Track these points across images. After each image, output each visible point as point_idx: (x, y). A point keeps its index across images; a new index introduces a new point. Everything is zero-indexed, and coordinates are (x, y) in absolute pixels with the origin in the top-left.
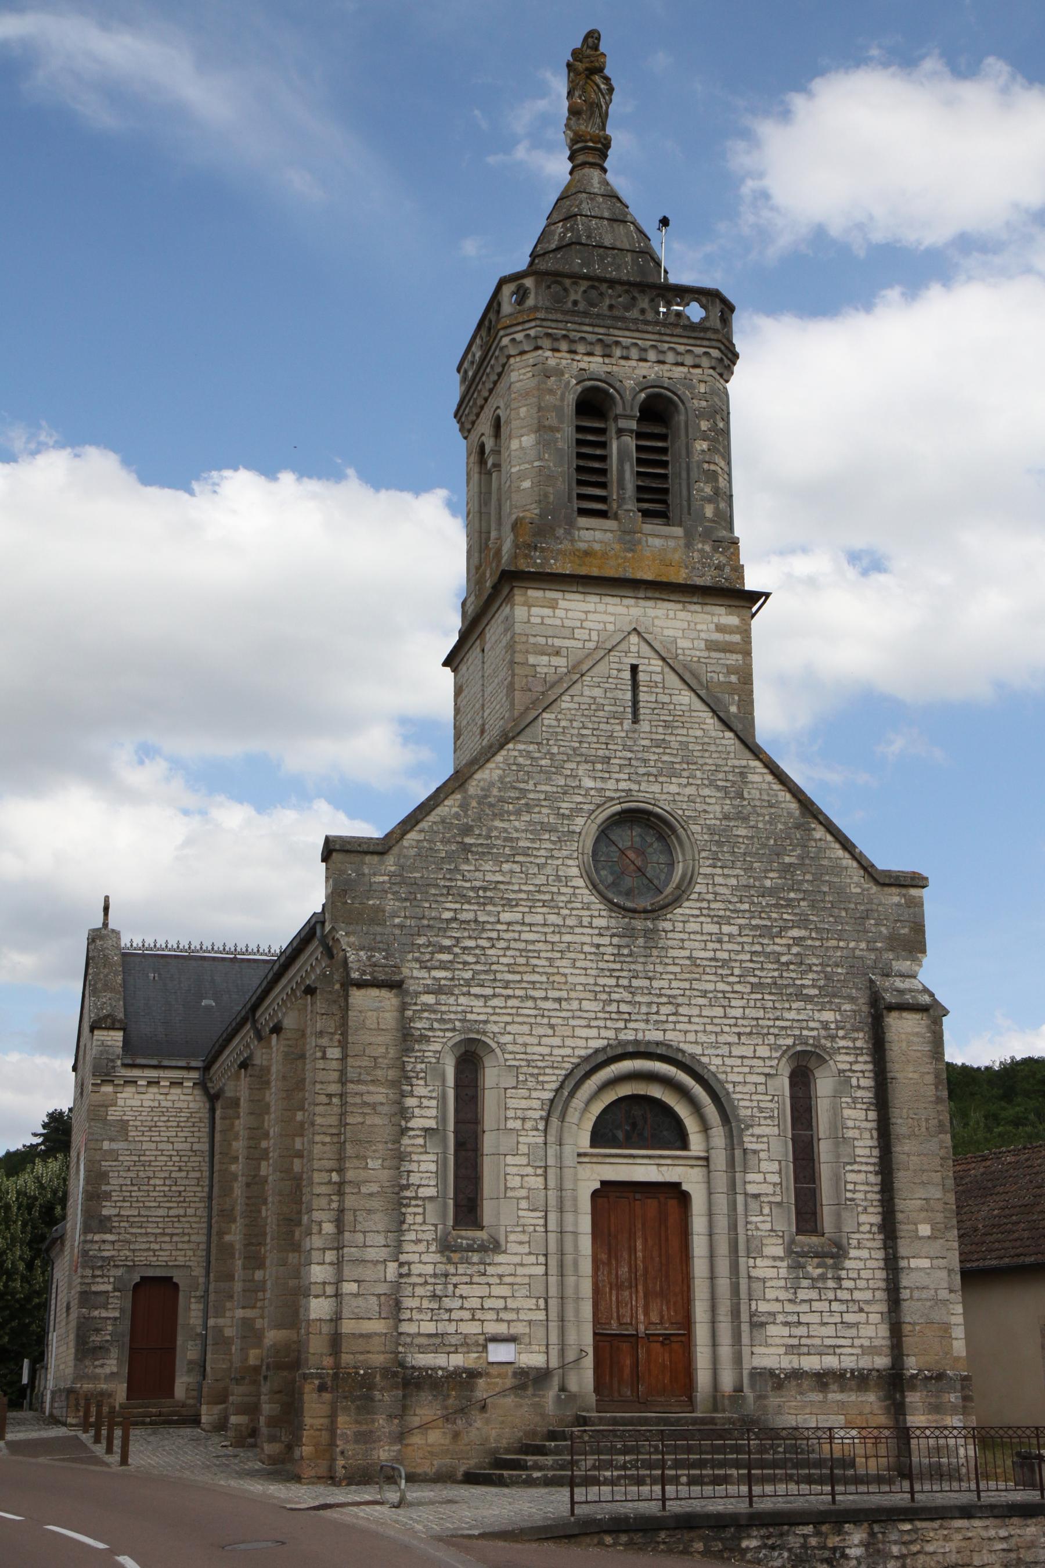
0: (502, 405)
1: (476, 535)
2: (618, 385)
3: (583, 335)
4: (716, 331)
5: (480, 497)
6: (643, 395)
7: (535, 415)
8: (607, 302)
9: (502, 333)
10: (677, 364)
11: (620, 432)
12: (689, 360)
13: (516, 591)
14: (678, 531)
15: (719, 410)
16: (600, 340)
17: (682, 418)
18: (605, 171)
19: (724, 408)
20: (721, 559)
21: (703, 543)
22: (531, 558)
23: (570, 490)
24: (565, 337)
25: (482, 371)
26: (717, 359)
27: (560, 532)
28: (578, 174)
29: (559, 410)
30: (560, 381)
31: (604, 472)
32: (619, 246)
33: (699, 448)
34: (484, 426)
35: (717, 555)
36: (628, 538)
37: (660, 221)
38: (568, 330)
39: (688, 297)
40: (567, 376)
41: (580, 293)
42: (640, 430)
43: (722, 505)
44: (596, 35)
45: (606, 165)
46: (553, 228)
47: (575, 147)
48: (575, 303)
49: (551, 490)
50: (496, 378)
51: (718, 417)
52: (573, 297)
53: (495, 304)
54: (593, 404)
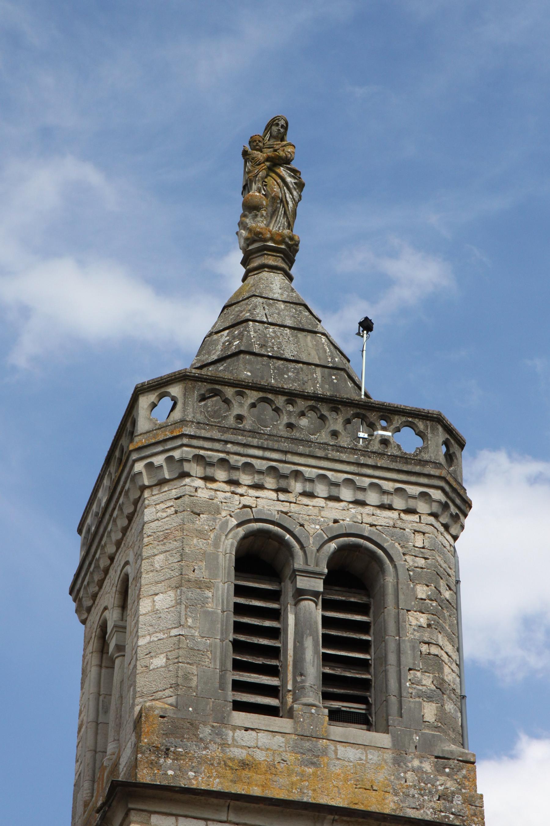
0: (131, 558)
1: (89, 755)
2: (297, 530)
3: (249, 460)
4: (437, 465)
5: (98, 700)
6: (333, 546)
7: (176, 566)
8: (285, 419)
9: (134, 456)
10: (382, 507)
11: (300, 594)
12: (399, 503)
13: (133, 816)
14: (384, 739)
15: (444, 577)
16: (272, 469)
17: (390, 579)
18: (291, 279)
19: (451, 572)
20: (449, 784)
21: (421, 758)
22: (160, 767)
23: (222, 678)
24: (223, 461)
25: (107, 516)
26: (439, 502)
27: (205, 732)
28: (251, 280)
29: (210, 559)
30: (214, 520)
31: (275, 653)
32: (305, 359)
33: (414, 622)
34: (109, 596)
35: (442, 779)
36: (307, 745)
37: (361, 324)
38: (228, 453)
39: (398, 420)
40: (224, 513)
41: (246, 407)
42: (328, 597)
43: (449, 707)
44: (282, 122)
45: (293, 272)
46: (215, 337)
47: (250, 248)
48: (240, 418)
49: (194, 669)
50: (126, 522)
51: (442, 583)
52: (236, 410)
53: (129, 425)
54: (261, 558)
